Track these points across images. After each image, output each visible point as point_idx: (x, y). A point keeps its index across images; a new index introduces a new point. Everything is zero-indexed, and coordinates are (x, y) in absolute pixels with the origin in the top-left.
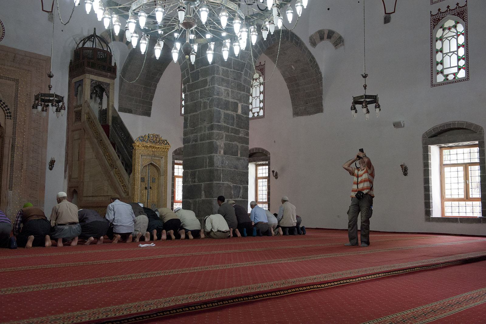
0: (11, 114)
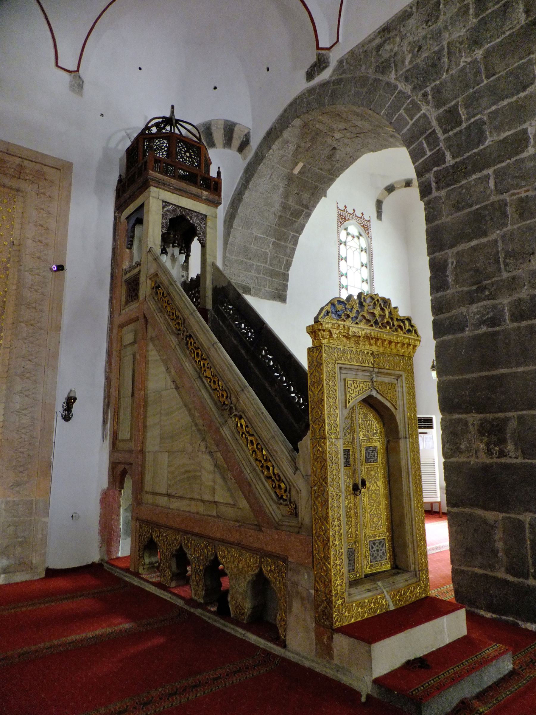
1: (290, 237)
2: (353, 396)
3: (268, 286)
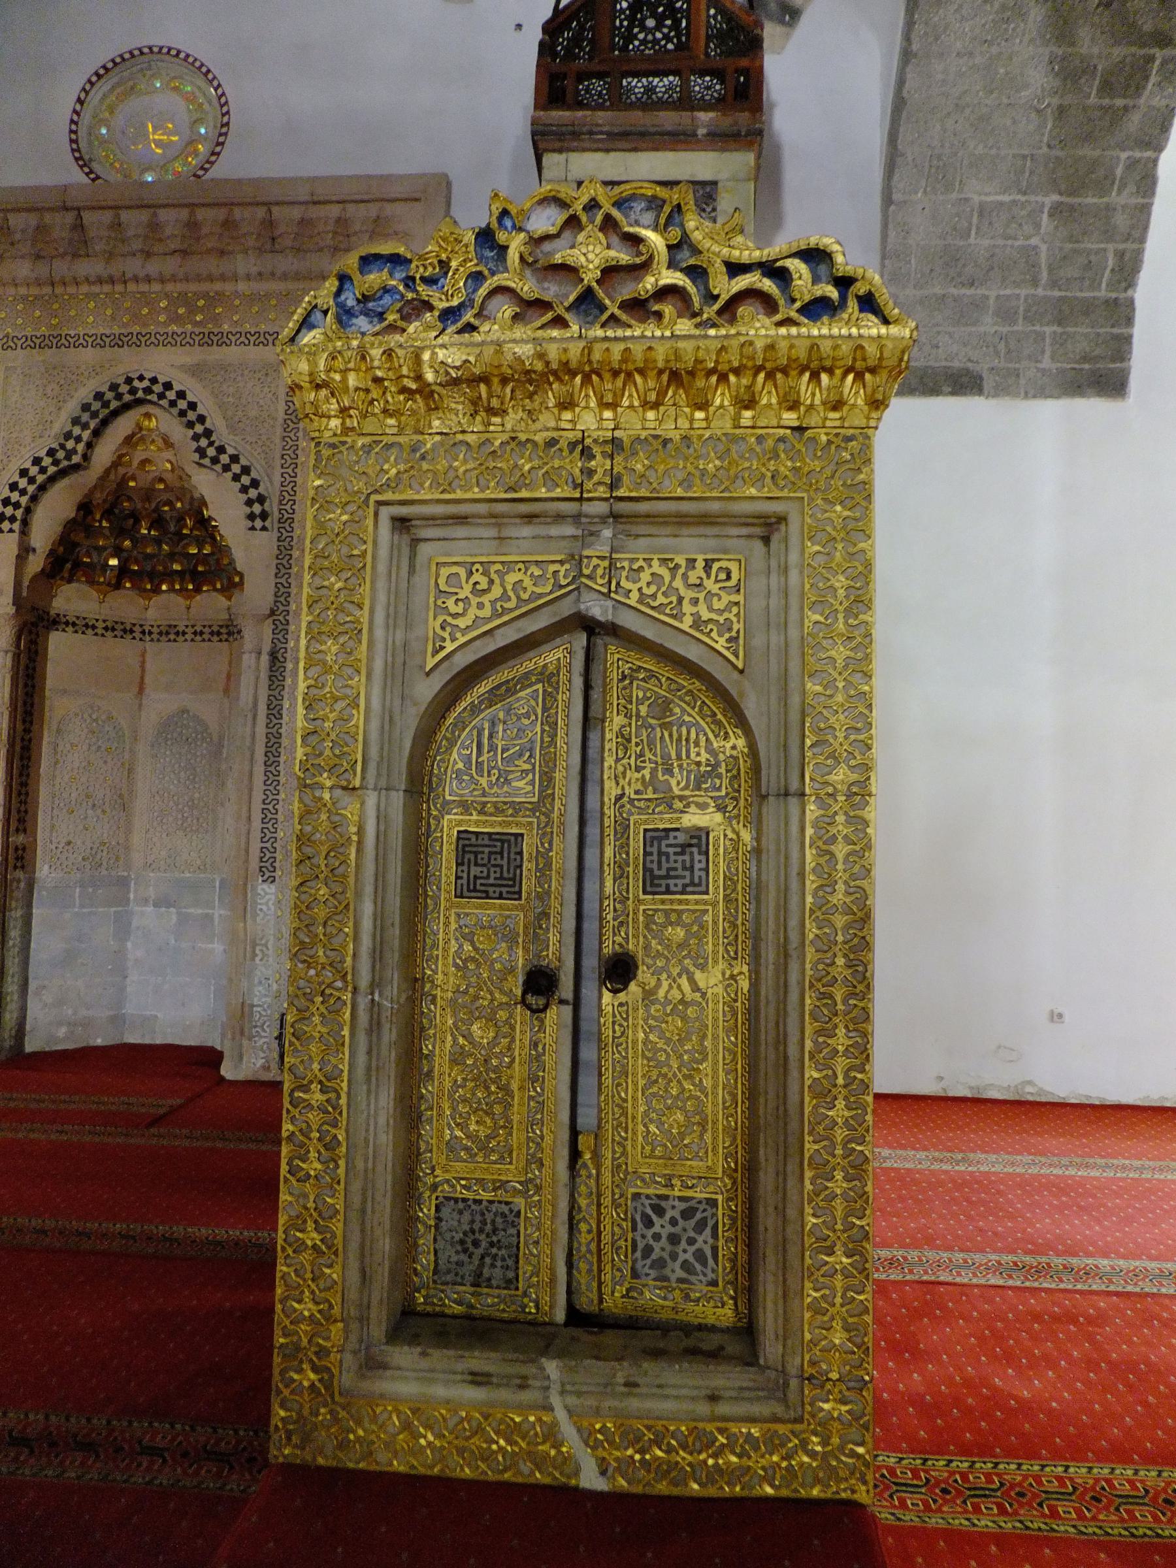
0: (266, 505)
1: (1119, 171)
2: (462, 623)
3: (1048, 354)
